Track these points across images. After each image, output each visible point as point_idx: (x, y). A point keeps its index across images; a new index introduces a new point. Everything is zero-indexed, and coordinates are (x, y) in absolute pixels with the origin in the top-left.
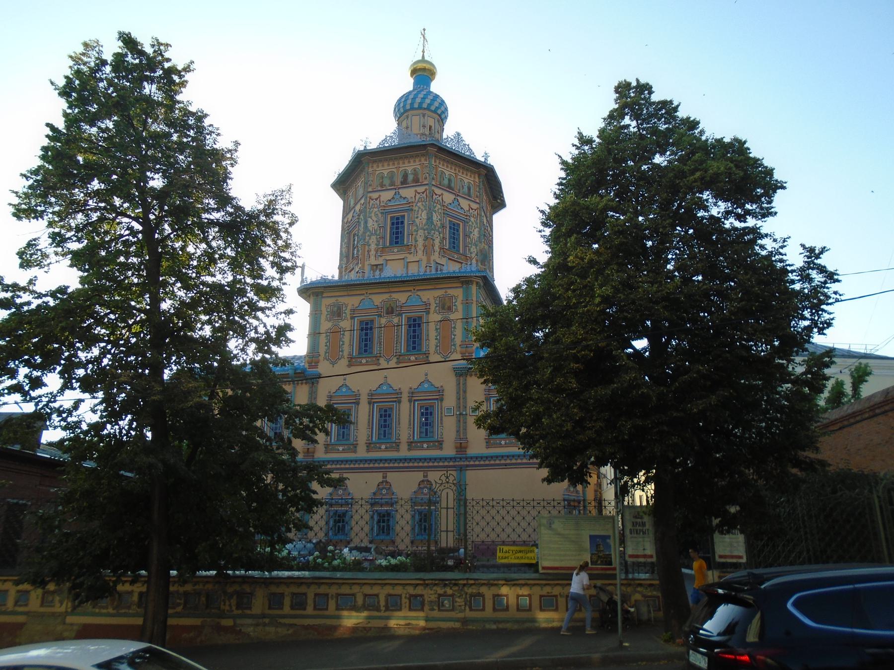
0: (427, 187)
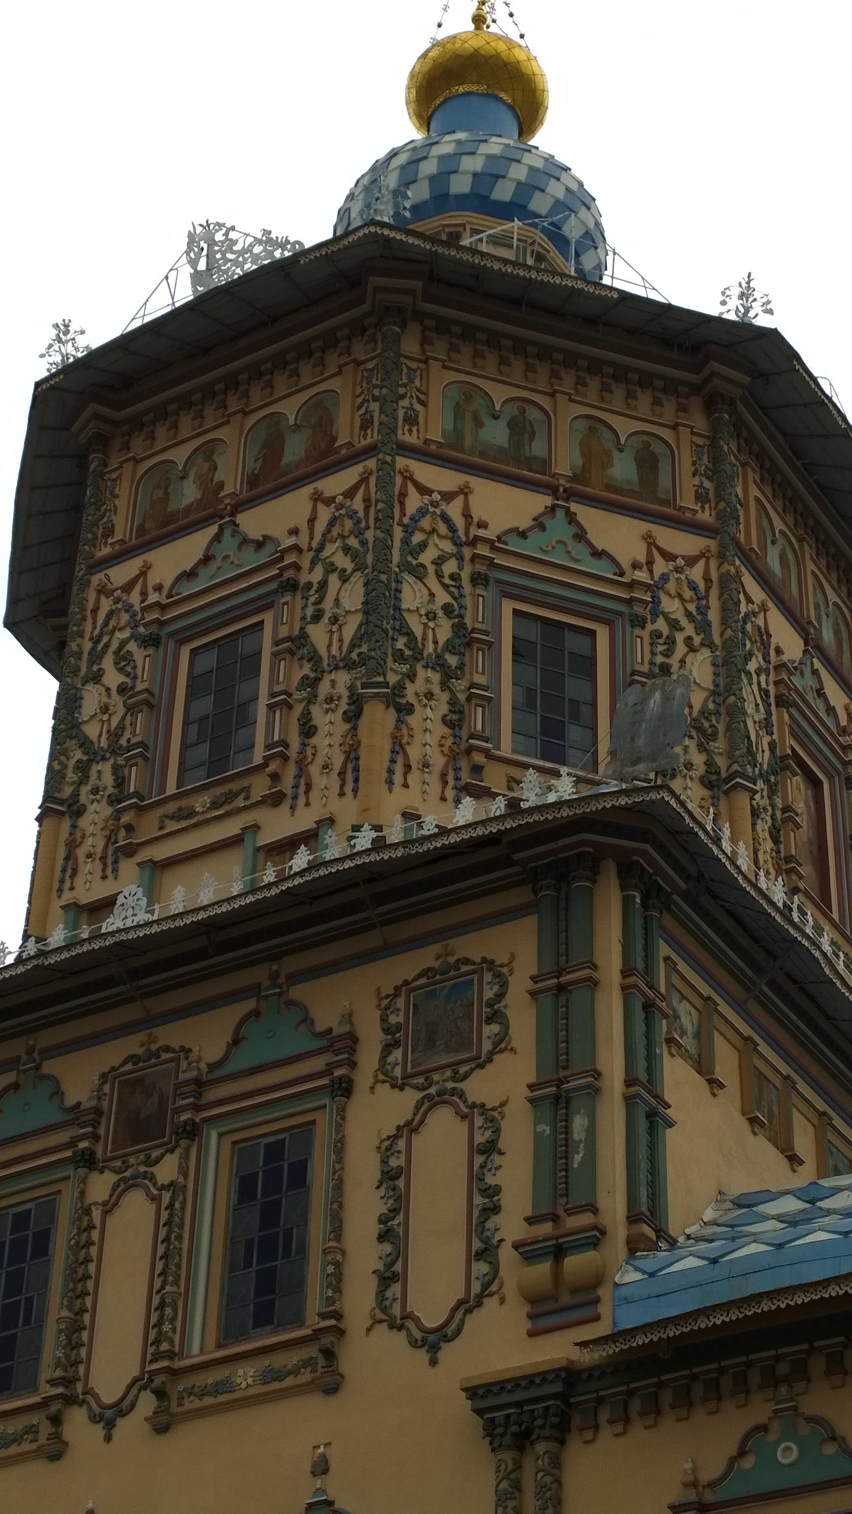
0: (372, 463)
